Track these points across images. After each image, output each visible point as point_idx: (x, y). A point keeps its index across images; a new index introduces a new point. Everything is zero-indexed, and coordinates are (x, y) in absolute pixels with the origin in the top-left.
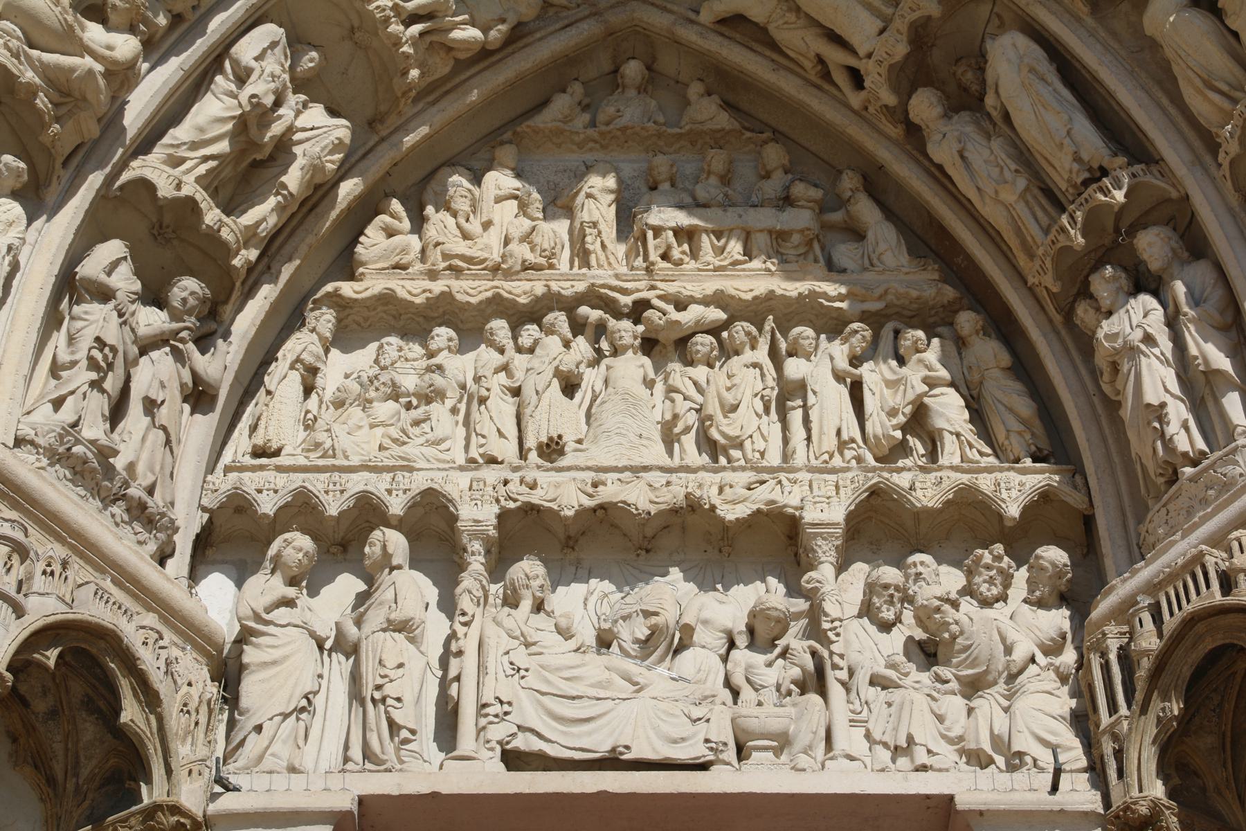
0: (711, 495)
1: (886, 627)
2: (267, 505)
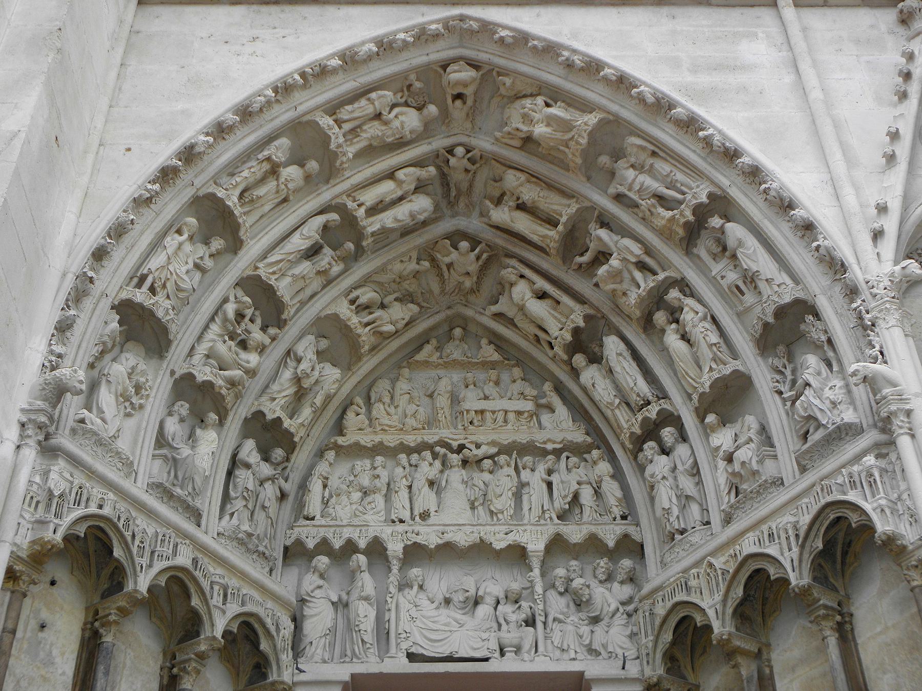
1: (561, 594)
2: (311, 544)
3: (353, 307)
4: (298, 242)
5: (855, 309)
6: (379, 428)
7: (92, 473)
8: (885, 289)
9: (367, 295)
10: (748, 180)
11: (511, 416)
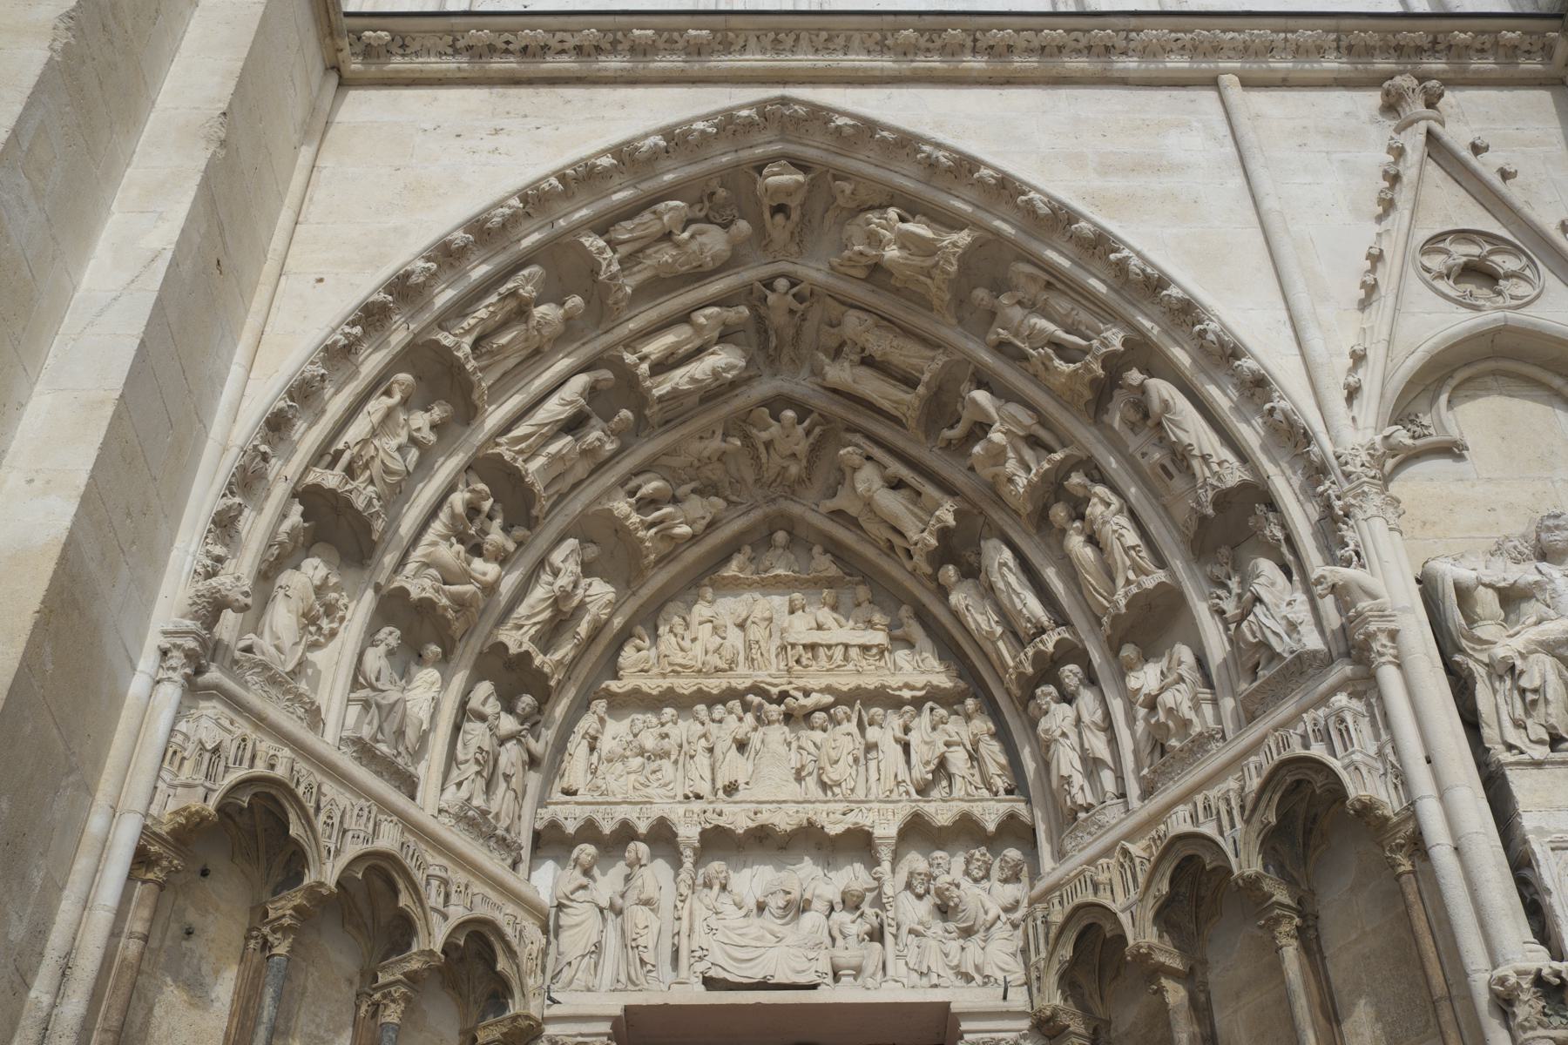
0: (821, 820)
1: (920, 897)
2: (571, 828)
3: (633, 500)
4: (554, 409)
5: (1322, 494)
6: (670, 669)
7: (261, 722)
8: (1363, 465)
9: (652, 486)
10: (1177, 321)
11: (854, 652)
